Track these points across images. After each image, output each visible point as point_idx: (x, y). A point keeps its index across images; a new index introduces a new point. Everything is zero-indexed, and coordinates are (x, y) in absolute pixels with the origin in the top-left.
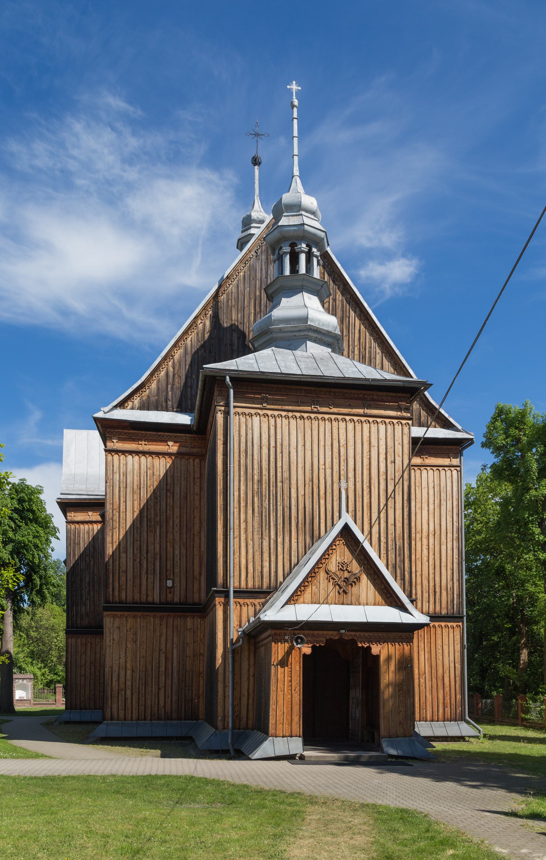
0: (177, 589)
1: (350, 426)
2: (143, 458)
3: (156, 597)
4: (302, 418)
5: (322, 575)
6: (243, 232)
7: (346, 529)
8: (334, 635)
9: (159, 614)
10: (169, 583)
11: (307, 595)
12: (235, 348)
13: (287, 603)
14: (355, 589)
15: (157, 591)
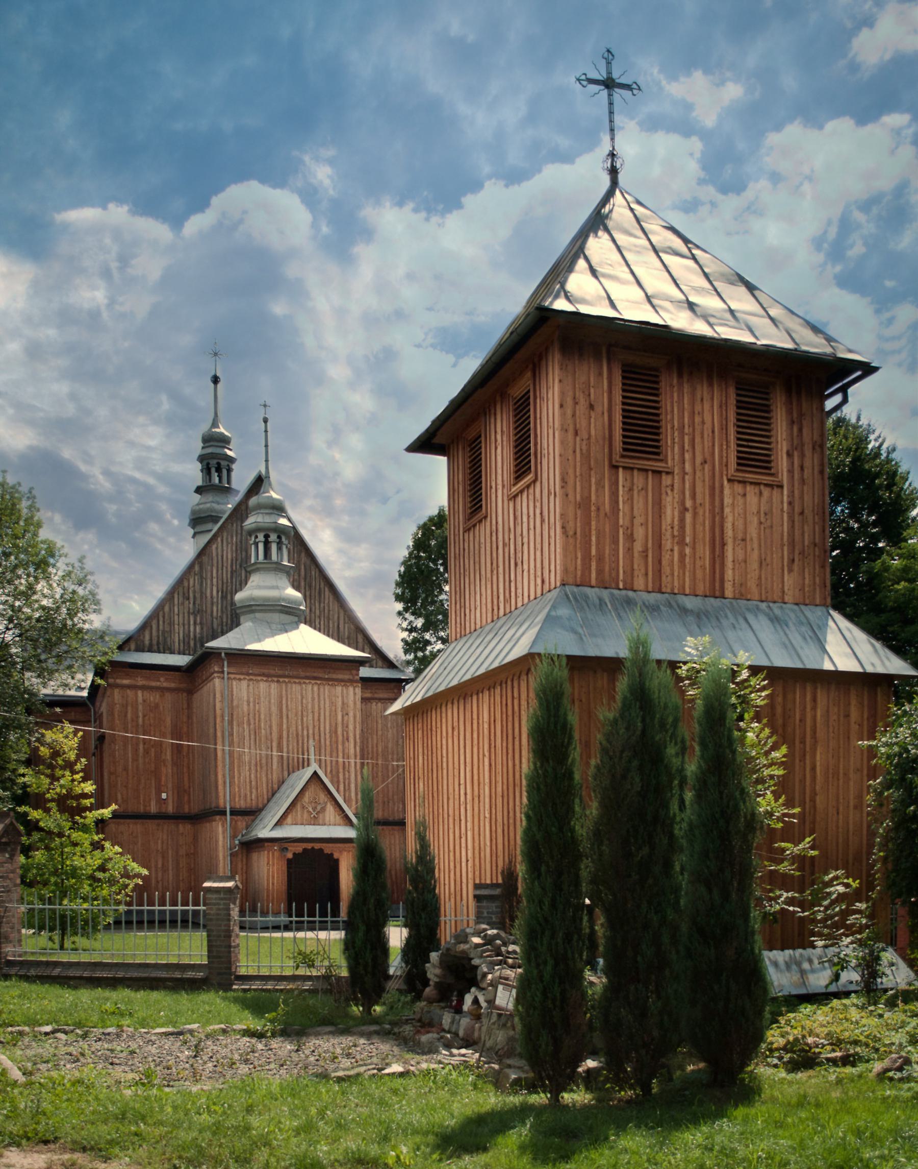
0: (170, 801)
1: (316, 688)
2: (140, 693)
3: (153, 809)
4: (278, 681)
5: (299, 807)
6: (203, 448)
7: (315, 773)
8: (309, 846)
9: (156, 821)
10: (164, 796)
11: (289, 819)
12: (215, 600)
13: (276, 825)
14: (321, 816)
15: (153, 803)
